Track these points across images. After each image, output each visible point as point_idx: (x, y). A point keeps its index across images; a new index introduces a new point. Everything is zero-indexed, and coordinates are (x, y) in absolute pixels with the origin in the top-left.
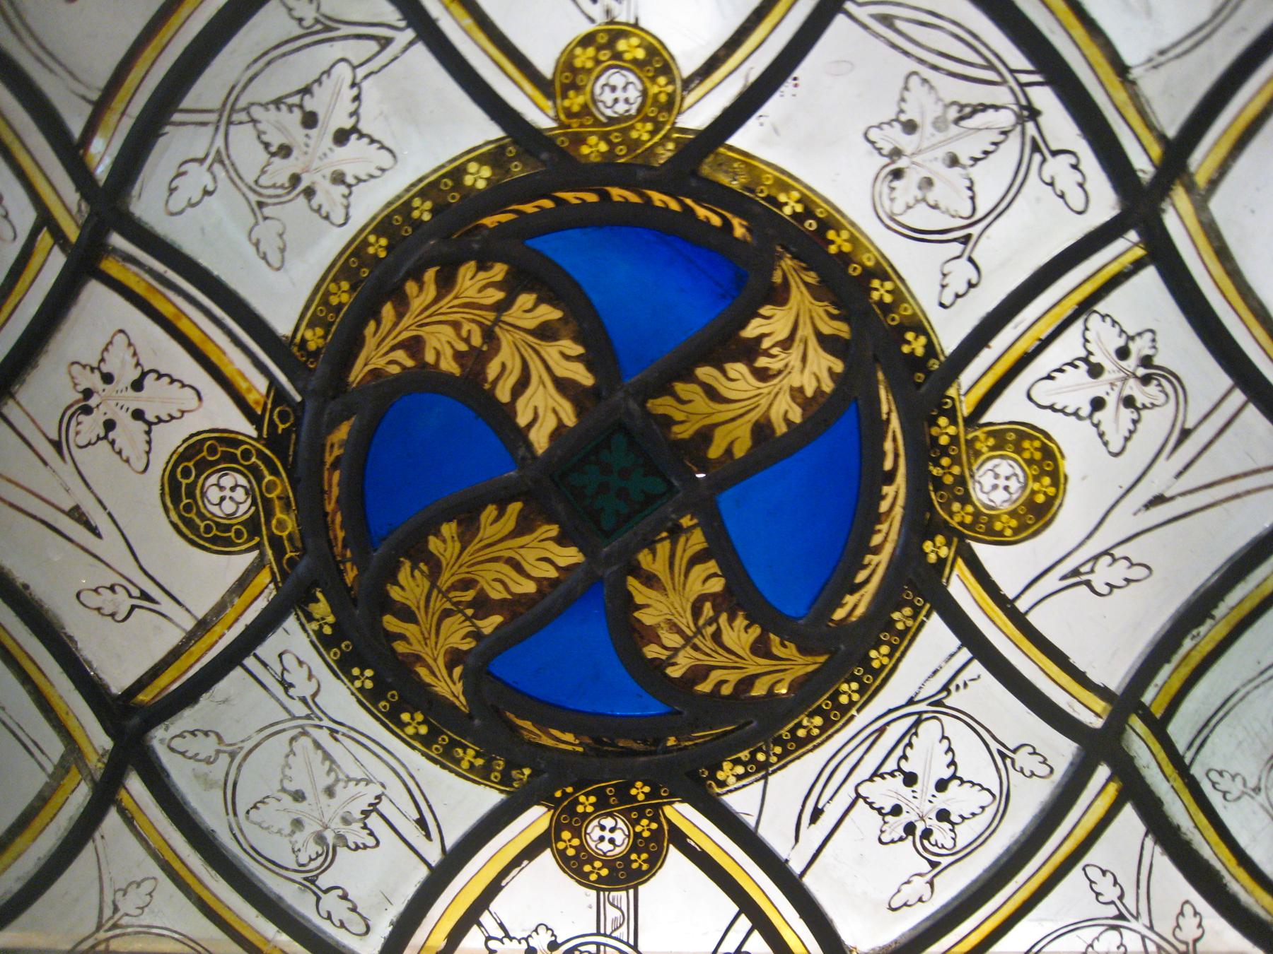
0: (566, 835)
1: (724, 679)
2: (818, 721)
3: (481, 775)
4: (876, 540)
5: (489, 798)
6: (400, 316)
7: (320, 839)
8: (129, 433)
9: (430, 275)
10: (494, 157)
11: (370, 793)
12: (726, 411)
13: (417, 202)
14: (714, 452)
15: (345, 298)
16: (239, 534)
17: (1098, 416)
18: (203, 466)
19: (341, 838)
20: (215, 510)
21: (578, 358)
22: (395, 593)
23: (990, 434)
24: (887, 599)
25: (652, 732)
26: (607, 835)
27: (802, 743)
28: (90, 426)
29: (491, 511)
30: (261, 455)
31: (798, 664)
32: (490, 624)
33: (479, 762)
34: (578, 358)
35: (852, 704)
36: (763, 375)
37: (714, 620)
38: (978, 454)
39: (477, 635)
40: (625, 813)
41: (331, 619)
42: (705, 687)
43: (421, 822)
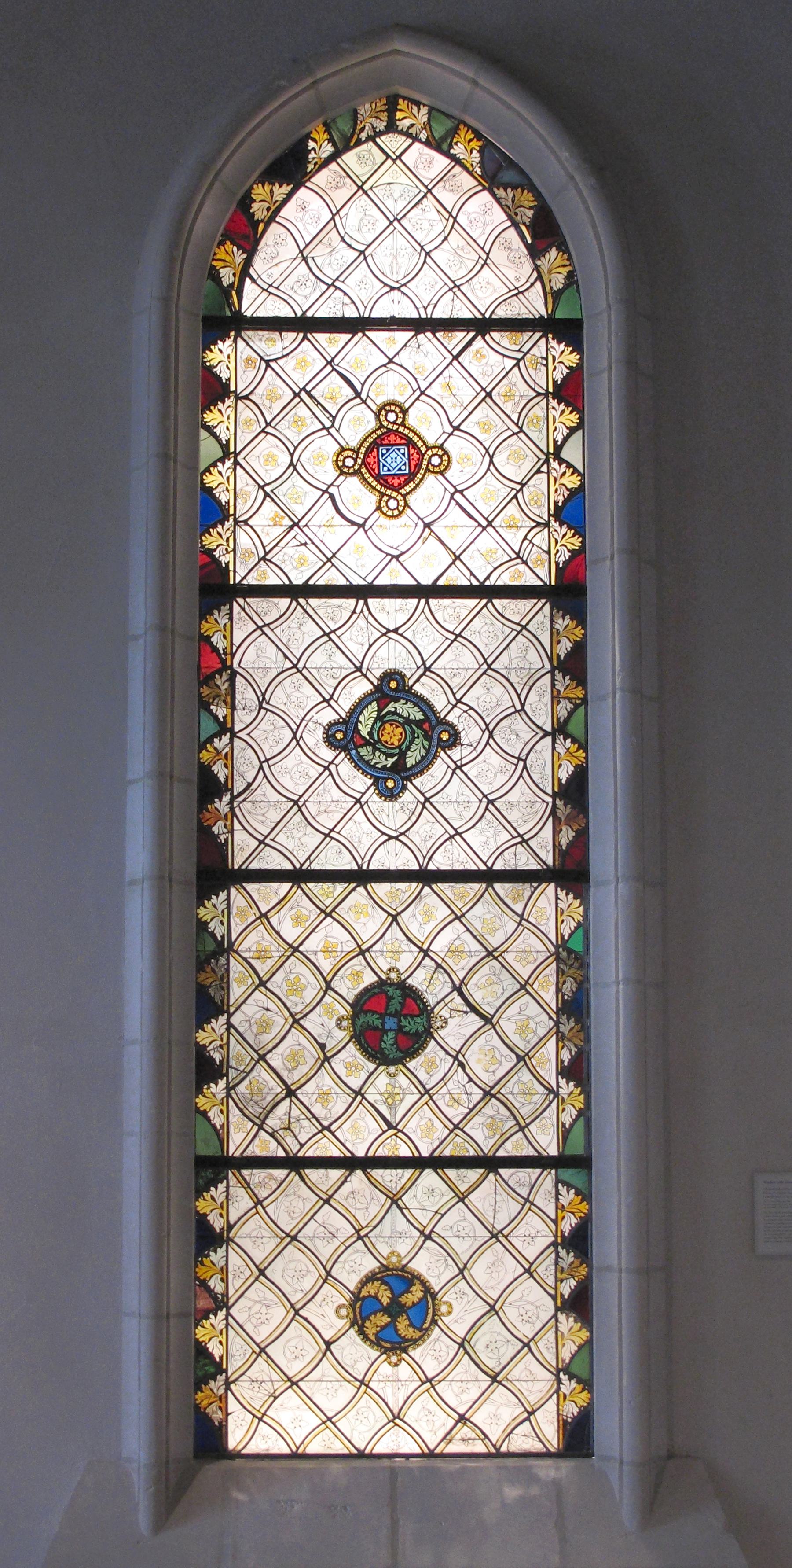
1: (409, 1336)
8: (330, 1304)
10: (379, 1268)
24: (430, 1325)
25: (399, 1343)
28: (325, 1303)
31: (418, 1334)
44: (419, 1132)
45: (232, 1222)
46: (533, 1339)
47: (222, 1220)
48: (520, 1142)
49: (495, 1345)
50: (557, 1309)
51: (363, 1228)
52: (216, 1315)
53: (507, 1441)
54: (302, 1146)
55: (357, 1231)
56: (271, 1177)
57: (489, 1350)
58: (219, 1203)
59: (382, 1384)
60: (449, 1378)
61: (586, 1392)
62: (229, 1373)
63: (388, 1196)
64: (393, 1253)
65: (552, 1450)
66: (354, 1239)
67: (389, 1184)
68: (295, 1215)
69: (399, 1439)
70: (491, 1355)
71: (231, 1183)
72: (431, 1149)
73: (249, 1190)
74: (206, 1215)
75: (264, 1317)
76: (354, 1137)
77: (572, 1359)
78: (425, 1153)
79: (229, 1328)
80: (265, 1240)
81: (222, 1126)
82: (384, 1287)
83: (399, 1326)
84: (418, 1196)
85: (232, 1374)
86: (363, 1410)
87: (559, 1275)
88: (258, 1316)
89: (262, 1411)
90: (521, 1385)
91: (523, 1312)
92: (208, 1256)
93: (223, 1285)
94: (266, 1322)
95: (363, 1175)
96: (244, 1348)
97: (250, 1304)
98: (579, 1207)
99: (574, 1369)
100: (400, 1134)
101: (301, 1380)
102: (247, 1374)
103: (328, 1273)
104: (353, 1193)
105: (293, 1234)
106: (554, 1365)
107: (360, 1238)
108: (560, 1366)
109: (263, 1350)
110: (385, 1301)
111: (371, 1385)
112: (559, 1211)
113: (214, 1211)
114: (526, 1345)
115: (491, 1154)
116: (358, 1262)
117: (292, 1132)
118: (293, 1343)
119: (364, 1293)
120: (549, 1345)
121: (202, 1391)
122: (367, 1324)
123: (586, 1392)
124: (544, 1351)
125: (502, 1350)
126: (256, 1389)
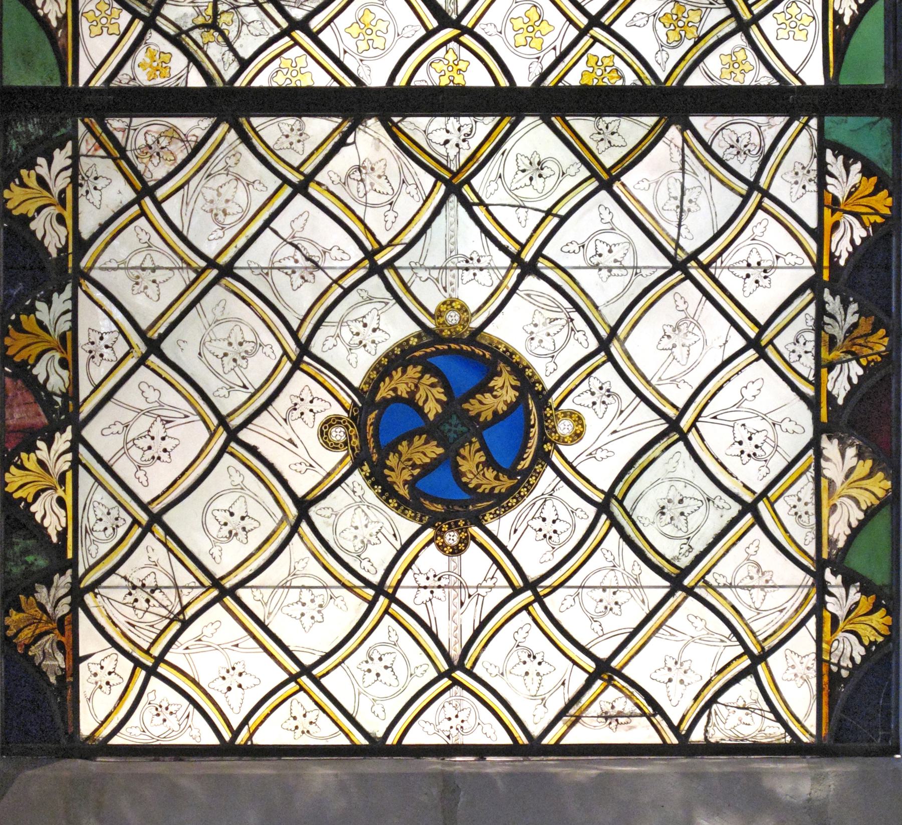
0: (439, 538)
1: (486, 488)
2: (515, 500)
3: (414, 518)
4: (529, 445)
5: (416, 526)
6: (391, 381)
7: (363, 542)
8: (308, 416)
9: (399, 370)
10: (418, 336)
11: (381, 525)
12: (483, 408)
13: (396, 349)
14: (482, 419)
15: (375, 376)
16: (341, 446)
17: (594, 407)
18: (331, 426)
19: (369, 541)
20: (334, 439)
21: (442, 393)
22: (388, 462)
23: (562, 413)
24: (534, 462)
25: (464, 504)
26: (452, 538)
27: (510, 508)
28: (296, 414)
29: (417, 437)
30: (349, 422)
31: (506, 483)
32: (418, 470)
33: (413, 515)
34: (442, 393)
35: (525, 495)
36: (495, 397)
37: (483, 469)
38: (559, 419)
39: (412, 475)
40: (457, 530)
41: (369, 471)
42: (480, 490)
43: (395, 535)
44: (510, 33)
45: (86, 235)
46: (764, 494)
47: (62, 231)
48: (741, 56)
49: (680, 508)
50: (820, 429)
51: (382, 248)
52: (50, 444)
53: (704, 719)
54: (244, 64)
55: (370, 255)
56: (174, 134)
57: (666, 518)
58: (56, 191)
59: (425, 594)
60: (575, 581)
61: (882, 612)
62: (81, 570)
63: (438, 178)
64: (449, 303)
65: (805, 739)
66: (361, 273)
67: (442, 150)
68: (229, 220)
69: (462, 716)
70: (669, 530)
71: (83, 149)
72: (537, 71)
73: (123, 164)
74: (26, 220)
75: (158, 446)
76: (363, 45)
77: (850, 539)
78: (524, 80)
79: (81, 470)
80: (159, 275)
81: (62, 20)
82: (428, 379)
83: (465, 466)
84: (508, 177)
85: (87, 572)
86: (383, 650)
87: (824, 354)
88: (144, 443)
89: (156, 651)
90: (738, 597)
91: (742, 435)
92: (32, 310)
93: (65, 374)
94: (164, 456)
95: (383, 132)
96: (114, 513)
97: (129, 416)
98: (872, 201)
99: (856, 562)
100: (466, 39)
101: (242, 584)
102: (122, 571)
103: (304, 348)
104: (359, 168)
105: (223, 260)
106: (811, 550)
107: (375, 270)
108: (825, 556)
109: (156, 519)
110: (432, 409)
111: (400, 595)
112: (827, 212)
113: (45, 212)
114: (749, 508)
115: (673, 82)
116: (372, 323)
117: (222, 33)
118: (223, 503)
119: (384, 392)
120: (801, 509)
121: (19, 610)
122: (392, 460)
123: (882, 612)
124: (790, 522)
125: (695, 520)
126: (142, 604)
